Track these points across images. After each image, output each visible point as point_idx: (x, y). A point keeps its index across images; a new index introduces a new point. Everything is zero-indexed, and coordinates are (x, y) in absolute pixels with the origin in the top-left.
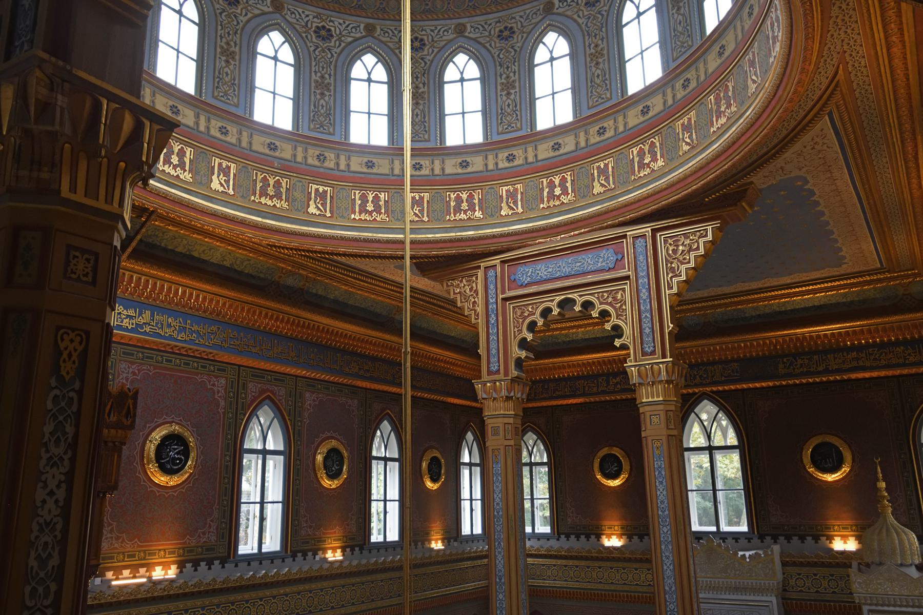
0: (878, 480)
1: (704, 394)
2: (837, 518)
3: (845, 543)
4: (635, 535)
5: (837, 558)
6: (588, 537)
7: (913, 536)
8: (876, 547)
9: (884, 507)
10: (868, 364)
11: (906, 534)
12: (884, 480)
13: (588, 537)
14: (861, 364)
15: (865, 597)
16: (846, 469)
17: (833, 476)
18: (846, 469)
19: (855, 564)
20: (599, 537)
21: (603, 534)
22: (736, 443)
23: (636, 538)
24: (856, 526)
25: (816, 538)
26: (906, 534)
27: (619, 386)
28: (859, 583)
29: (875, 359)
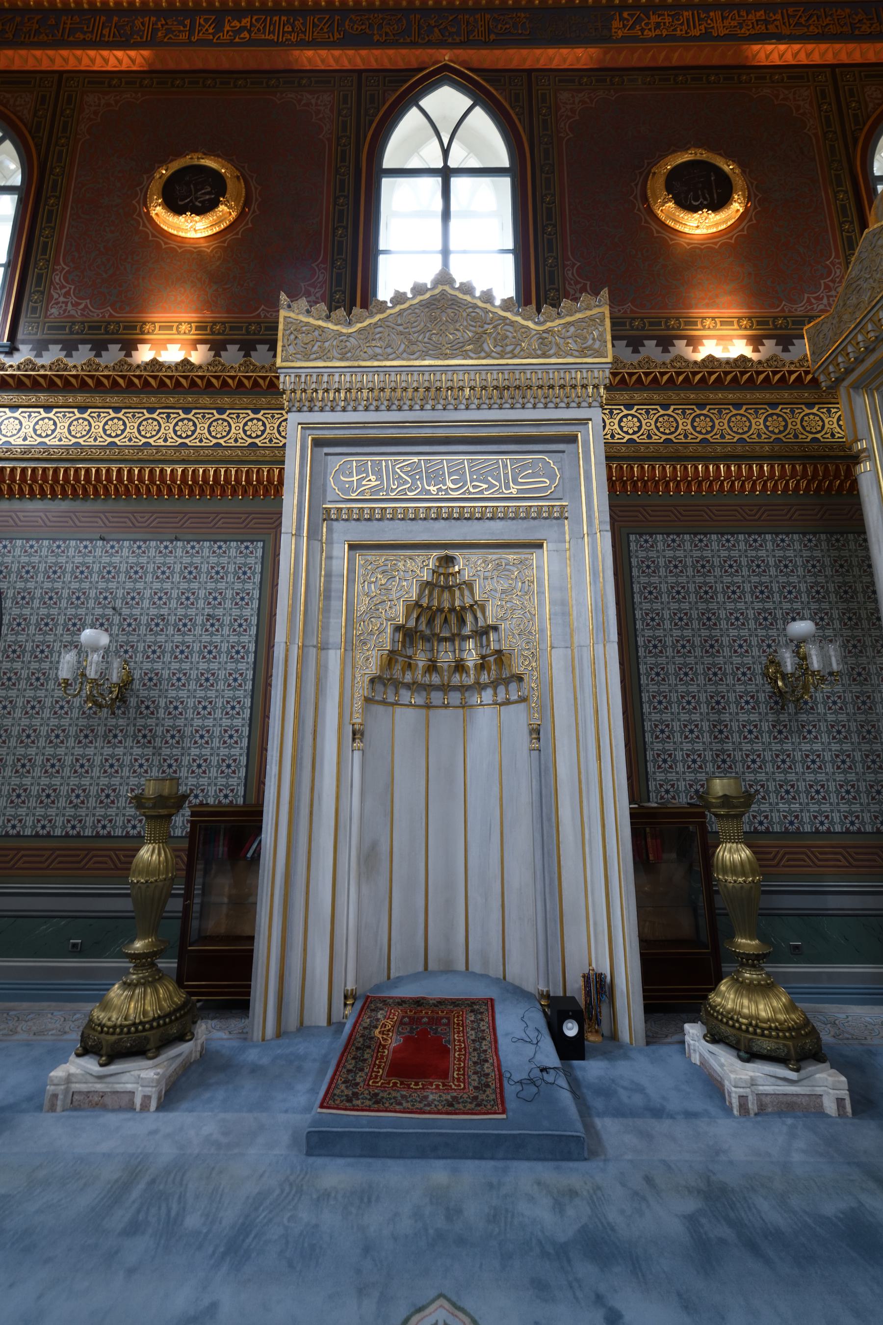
1: (446, 68)
2: (707, 306)
4: (233, 342)
6: (99, 347)
10: (786, 31)
13: (99, 347)
14: (772, 29)
16: (736, 208)
18: (736, 208)
20: (130, 346)
21: (143, 341)
22: (505, 163)
23: (233, 349)
24: (750, 318)
25: (666, 343)
27: (245, 35)
29: (798, 24)
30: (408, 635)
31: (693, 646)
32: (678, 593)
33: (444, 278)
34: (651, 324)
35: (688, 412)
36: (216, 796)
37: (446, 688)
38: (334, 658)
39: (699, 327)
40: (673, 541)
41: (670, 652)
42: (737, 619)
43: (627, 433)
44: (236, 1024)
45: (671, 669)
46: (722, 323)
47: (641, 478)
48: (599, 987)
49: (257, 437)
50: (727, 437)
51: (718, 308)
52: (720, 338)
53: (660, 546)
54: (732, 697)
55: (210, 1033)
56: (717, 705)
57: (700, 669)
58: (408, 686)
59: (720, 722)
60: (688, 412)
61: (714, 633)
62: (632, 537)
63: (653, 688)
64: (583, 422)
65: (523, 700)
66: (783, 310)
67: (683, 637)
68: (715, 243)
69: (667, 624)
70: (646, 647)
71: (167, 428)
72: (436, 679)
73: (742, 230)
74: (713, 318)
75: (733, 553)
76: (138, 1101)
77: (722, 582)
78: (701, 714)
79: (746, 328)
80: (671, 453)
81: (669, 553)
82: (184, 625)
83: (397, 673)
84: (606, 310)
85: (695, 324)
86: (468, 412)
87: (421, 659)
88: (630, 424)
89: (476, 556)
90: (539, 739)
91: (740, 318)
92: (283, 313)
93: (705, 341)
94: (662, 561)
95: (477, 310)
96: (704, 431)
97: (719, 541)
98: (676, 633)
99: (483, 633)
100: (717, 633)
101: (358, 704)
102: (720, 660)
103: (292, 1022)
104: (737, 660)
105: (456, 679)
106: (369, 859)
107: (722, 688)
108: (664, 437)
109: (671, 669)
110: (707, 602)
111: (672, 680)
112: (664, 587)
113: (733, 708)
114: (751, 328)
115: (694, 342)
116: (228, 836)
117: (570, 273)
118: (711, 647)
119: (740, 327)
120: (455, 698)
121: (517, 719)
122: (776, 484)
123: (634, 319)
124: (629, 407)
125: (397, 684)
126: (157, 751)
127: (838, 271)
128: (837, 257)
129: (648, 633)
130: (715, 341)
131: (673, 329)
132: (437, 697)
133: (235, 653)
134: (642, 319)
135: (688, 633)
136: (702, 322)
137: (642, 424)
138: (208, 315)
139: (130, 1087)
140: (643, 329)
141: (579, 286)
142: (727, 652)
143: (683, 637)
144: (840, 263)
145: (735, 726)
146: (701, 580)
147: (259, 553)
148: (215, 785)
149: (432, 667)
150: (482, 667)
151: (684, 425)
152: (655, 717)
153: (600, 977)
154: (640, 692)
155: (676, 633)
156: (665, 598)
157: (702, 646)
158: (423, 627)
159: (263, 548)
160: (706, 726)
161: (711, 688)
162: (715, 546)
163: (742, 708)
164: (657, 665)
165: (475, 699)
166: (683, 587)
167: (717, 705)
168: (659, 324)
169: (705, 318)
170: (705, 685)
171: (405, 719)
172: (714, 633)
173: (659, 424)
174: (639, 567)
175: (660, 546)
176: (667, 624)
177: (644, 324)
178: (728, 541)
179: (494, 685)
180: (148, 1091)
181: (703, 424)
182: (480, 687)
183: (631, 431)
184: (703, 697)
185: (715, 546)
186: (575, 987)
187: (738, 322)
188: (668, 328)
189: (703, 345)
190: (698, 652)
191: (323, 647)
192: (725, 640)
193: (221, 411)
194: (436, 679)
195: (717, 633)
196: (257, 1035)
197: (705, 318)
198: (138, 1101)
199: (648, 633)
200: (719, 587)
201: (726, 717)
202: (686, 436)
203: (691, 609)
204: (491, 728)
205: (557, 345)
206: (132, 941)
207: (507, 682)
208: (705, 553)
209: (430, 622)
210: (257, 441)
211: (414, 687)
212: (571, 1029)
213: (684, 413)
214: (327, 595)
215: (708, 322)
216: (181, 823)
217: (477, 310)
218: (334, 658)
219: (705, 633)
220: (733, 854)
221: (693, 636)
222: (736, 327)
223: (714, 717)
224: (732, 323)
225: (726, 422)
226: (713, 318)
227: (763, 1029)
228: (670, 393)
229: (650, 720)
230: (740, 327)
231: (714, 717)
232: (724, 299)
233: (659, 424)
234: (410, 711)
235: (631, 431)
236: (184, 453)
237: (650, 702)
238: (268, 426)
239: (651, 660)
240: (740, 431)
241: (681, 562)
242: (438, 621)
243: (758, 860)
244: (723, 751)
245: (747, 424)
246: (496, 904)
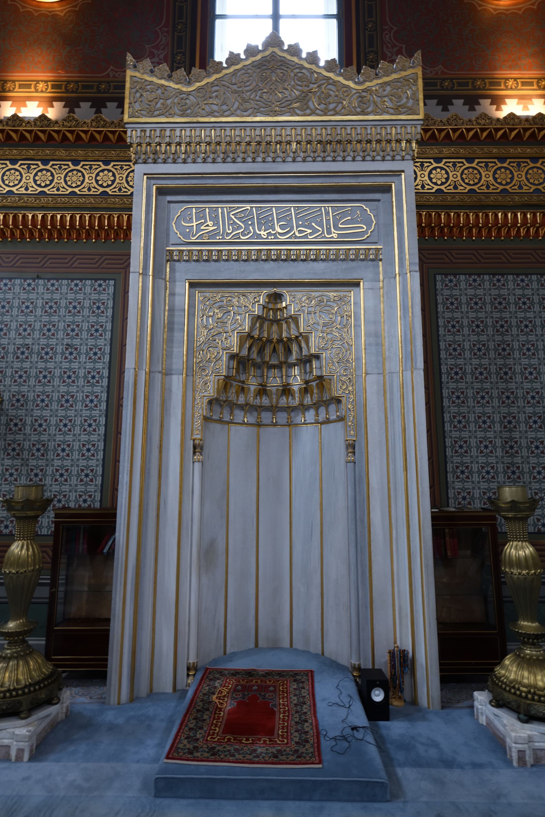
2: (511, 68)
4: (85, 100)
23: (85, 106)
25: (472, 102)
30: (240, 362)
31: (489, 373)
32: (478, 326)
33: (274, 40)
34: (459, 84)
35: (426, 165)
36: (77, 501)
37: (274, 409)
38: (177, 383)
40: (475, 281)
41: (469, 378)
42: (529, 350)
43: (436, 184)
44: (96, 691)
45: (470, 392)
46: (523, 84)
47: (447, 225)
48: (403, 661)
49: (108, 186)
50: (525, 187)
51: (520, 70)
52: (521, 98)
53: (463, 285)
54: (522, 417)
55: (73, 698)
56: (509, 424)
57: (495, 393)
58: (241, 407)
59: (511, 438)
60: (490, 165)
61: (508, 362)
62: (438, 277)
63: (454, 409)
64: (397, 173)
65: (341, 419)
67: (481, 365)
68: (520, 9)
69: (467, 354)
70: (448, 374)
71: (28, 178)
72: (265, 401)
74: (515, 79)
75: (526, 292)
76: (13, 753)
77: (516, 317)
78: (495, 432)
80: (477, 202)
81: (471, 292)
82: (47, 353)
83: (232, 395)
84: (419, 71)
85: (499, 84)
86: (295, 164)
87: (253, 384)
88: (439, 176)
89: (301, 294)
90: (354, 453)
92: (129, 73)
93: (507, 101)
94: (464, 299)
95: (304, 71)
96: (504, 182)
97: (514, 281)
98: (475, 362)
99: (306, 361)
100: (510, 362)
101: (198, 423)
102: (513, 385)
103: (143, 689)
104: (527, 385)
105: (283, 402)
106: (208, 555)
107: (514, 410)
108: (469, 188)
109: (470, 392)
110: (502, 334)
111: (471, 402)
112: (465, 322)
113: (523, 427)
115: (498, 101)
116: (87, 535)
117: (387, 37)
118: (505, 374)
120: (282, 417)
121: (336, 435)
122: (537, 232)
123: (444, 80)
124: (438, 160)
125: (232, 406)
126: (25, 462)
129: (451, 362)
131: (479, 89)
132: (266, 417)
133: (91, 378)
134: (452, 80)
135: (485, 361)
136: (505, 83)
137: (448, 176)
138: (63, 75)
139: (6, 742)
140: (452, 89)
141: (395, 49)
142: (519, 378)
143: (481, 365)
145: (524, 442)
146: (498, 315)
147: (111, 290)
148: (77, 492)
149: (262, 391)
150: (306, 390)
151: (487, 177)
152: (455, 434)
153: (403, 654)
154: (443, 413)
155: (475, 362)
156: (466, 331)
157: (497, 373)
158: (254, 355)
159: (115, 285)
160: (498, 442)
161: (504, 410)
162: (511, 285)
163: (531, 427)
164: (457, 389)
165: (300, 419)
166: (482, 322)
167: (509, 424)
168: (467, 84)
169: (507, 79)
170: (499, 407)
171: (239, 436)
172: (508, 362)
173: (464, 176)
174: (444, 304)
175: (463, 285)
176: (467, 354)
177: (453, 84)
178: (522, 281)
179: (316, 406)
180: (22, 745)
181: (503, 176)
182: (303, 408)
183: (439, 182)
184: (497, 417)
185: (511, 285)
186: (382, 661)
187: (538, 83)
188: (474, 88)
189: (505, 103)
190: (494, 378)
191: (167, 373)
192: (518, 368)
193: (76, 162)
194: (265, 401)
195: (510, 362)
196: (114, 700)
197: (507, 79)
198: (13, 753)
199: (451, 362)
200: (514, 322)
201: (516, 435)
202: (488, 187)
203: (488, 341)
204: (313, 442)
205: (375, 103)
206: (6, 622)
207: (327, 403)
208: (502, 292)
209: (261, 351)
210: (108, 190)
211: (247, 407)
212: (378, 696)
213: (487, 166)
214: (171, 327)
215: (510, 83)
216: (46, 523)
217: (304, 71)
218: (177, 383)
219: (500, 362)
220: (519, 550)
221: (490, 364)
223: (506, 435)
224: (531, 84)
225: (523, 174)
226: (515, 79)
227: (540, 696)
228: (475, 148)
229: (451, 437)
230: (539, 88)
231: (506, 435)
233: (464, 176)
234: (243, 428)
235: (439, 182)
236: (44, 200)
237: (451, 422)
238: (117, 176)
239: (452, 385)
240: (536, 182)
241: (480, 299)
242: (268, 351)
243: (540, 556)
244: (513, 464)
245: (478, 176)
246: (316, 592)
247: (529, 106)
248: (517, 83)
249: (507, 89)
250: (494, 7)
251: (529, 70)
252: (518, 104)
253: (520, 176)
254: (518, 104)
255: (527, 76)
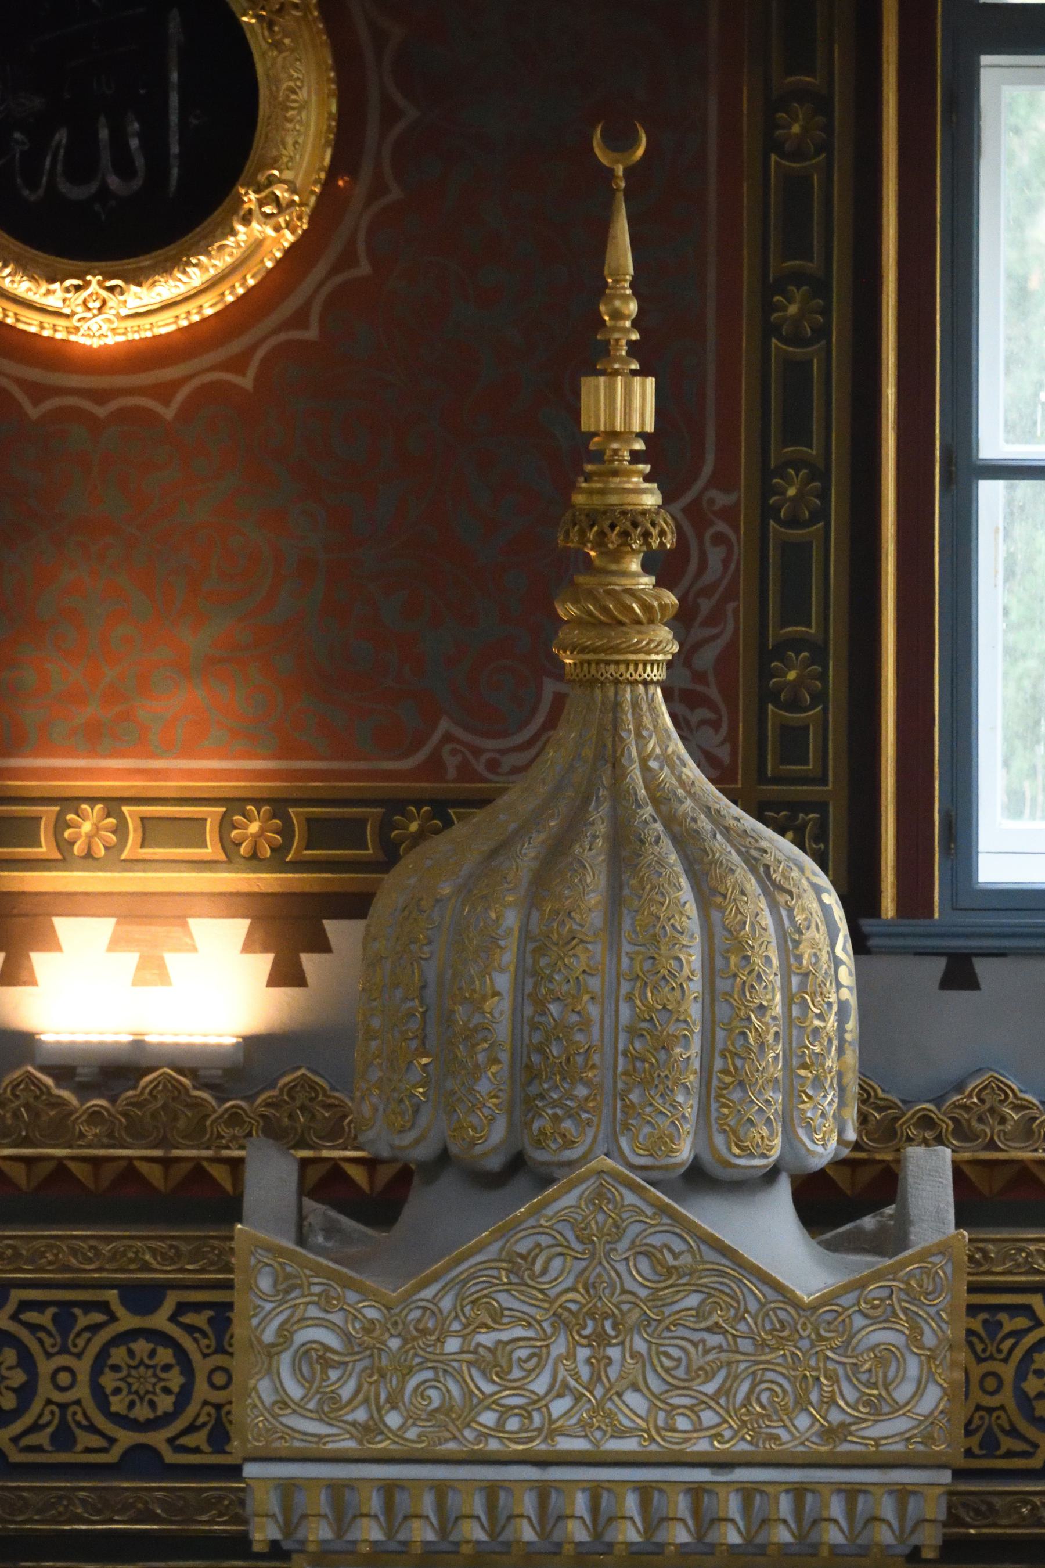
0: (590, 355)
2: (95, 738)
3: (151, 970)
5: (60, 1129)
7: (818, 896)
8: (500, 1010)
9: (615, 620)
11: (773, 888)
12: (648, 358)
15: (337, 1489)
17: (139, 296)
18: (259, 236)
19: (270, 1179)
24: (277, 806)
26: (773, 888)
28: (318, 1359)
39: (45, 849)
50: (86, 1440)
52: (136, 912)
66: (434, 767)
68: (164, 392)
73: (299, 320)
79: (254, 861)
85: (23, 831)
91: (234, 804)
93: (62, 925)
114: (278, 861)
119: (230, 847)
127: (715, 556)
128: (724, 479)
130: (106, 926)
136: (60, 825)
144: (729, 514)
169: (70, 802)
187: (226, 824)
197: (70, 802)
215: (87, 824)
222: (211, 850)
224: (189, 831)
226: (113, 804)
230: (231, 855)
232: (172, 702)
240: (142, 1412)
247: (173, 960)
248: (120, 830)
249: (64, 860)
250: (34, 374)
251: (188, 752)
252: (116, 944)
253: (64, 1378)
254: (116, 944)
255: (172, 786)
